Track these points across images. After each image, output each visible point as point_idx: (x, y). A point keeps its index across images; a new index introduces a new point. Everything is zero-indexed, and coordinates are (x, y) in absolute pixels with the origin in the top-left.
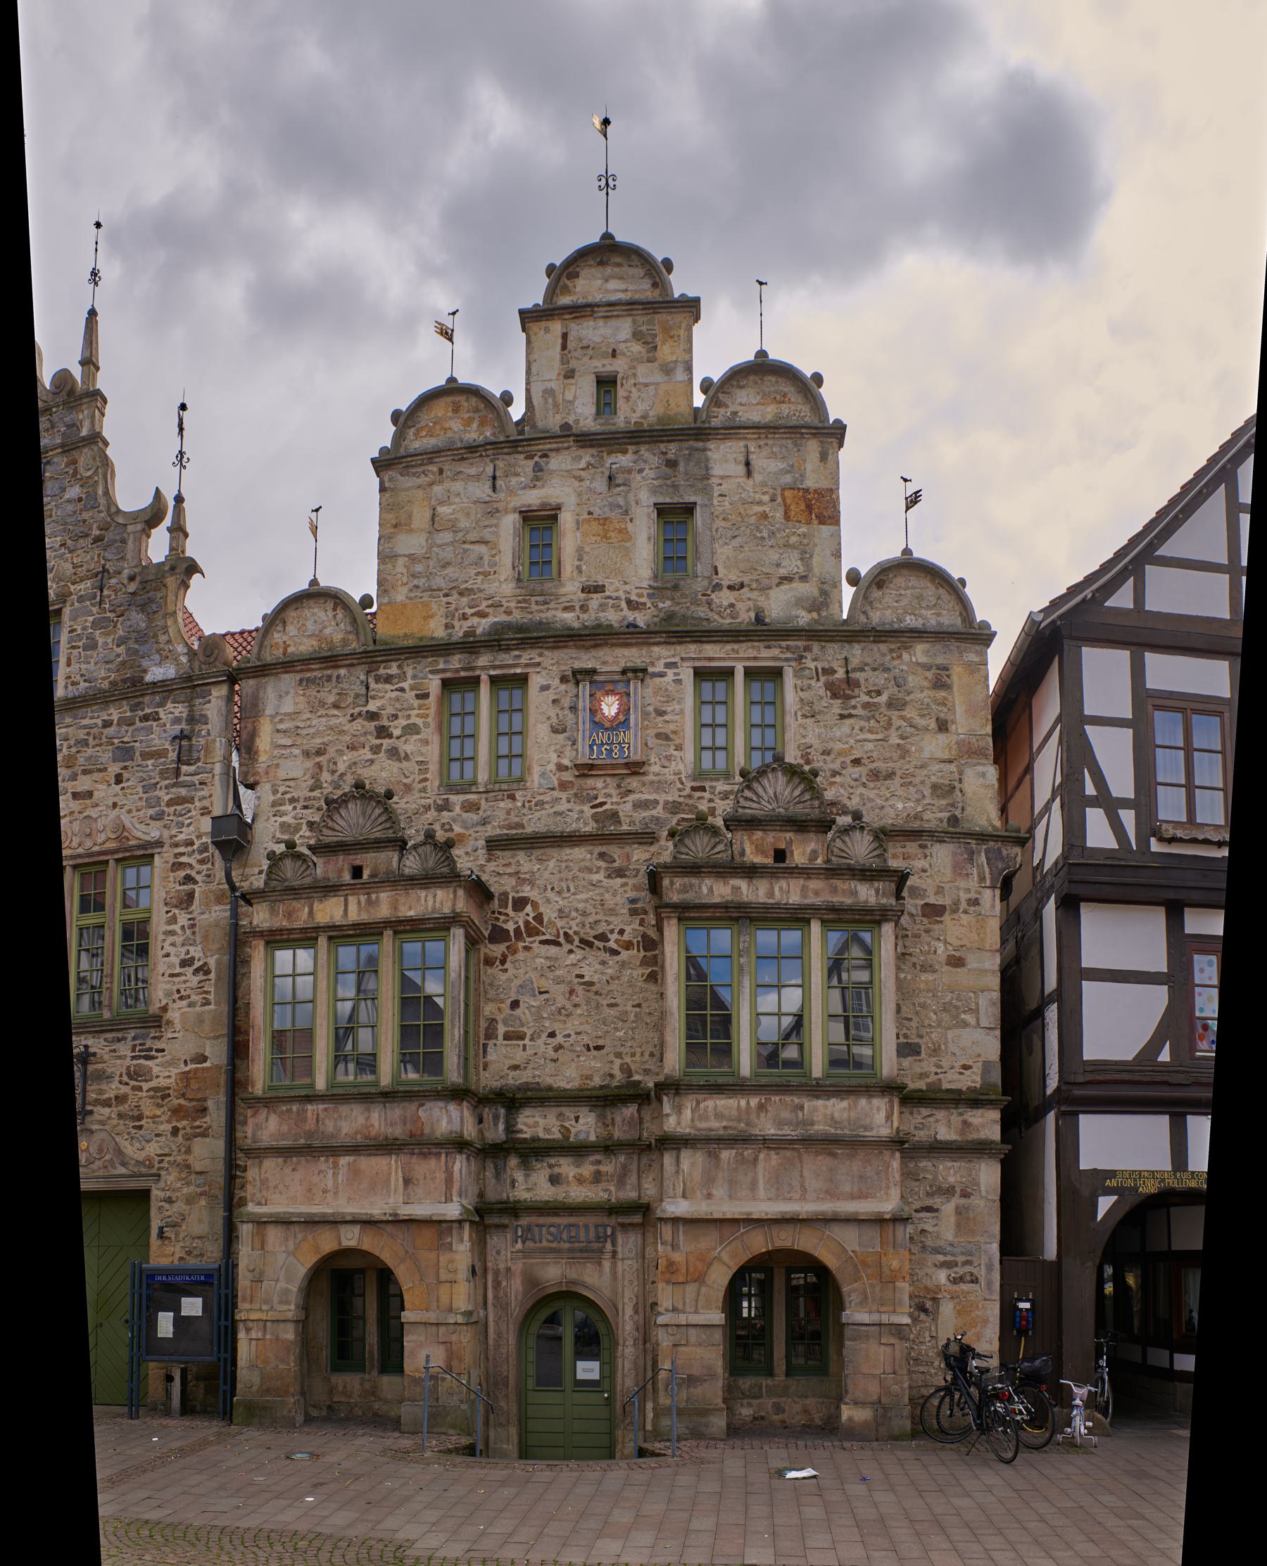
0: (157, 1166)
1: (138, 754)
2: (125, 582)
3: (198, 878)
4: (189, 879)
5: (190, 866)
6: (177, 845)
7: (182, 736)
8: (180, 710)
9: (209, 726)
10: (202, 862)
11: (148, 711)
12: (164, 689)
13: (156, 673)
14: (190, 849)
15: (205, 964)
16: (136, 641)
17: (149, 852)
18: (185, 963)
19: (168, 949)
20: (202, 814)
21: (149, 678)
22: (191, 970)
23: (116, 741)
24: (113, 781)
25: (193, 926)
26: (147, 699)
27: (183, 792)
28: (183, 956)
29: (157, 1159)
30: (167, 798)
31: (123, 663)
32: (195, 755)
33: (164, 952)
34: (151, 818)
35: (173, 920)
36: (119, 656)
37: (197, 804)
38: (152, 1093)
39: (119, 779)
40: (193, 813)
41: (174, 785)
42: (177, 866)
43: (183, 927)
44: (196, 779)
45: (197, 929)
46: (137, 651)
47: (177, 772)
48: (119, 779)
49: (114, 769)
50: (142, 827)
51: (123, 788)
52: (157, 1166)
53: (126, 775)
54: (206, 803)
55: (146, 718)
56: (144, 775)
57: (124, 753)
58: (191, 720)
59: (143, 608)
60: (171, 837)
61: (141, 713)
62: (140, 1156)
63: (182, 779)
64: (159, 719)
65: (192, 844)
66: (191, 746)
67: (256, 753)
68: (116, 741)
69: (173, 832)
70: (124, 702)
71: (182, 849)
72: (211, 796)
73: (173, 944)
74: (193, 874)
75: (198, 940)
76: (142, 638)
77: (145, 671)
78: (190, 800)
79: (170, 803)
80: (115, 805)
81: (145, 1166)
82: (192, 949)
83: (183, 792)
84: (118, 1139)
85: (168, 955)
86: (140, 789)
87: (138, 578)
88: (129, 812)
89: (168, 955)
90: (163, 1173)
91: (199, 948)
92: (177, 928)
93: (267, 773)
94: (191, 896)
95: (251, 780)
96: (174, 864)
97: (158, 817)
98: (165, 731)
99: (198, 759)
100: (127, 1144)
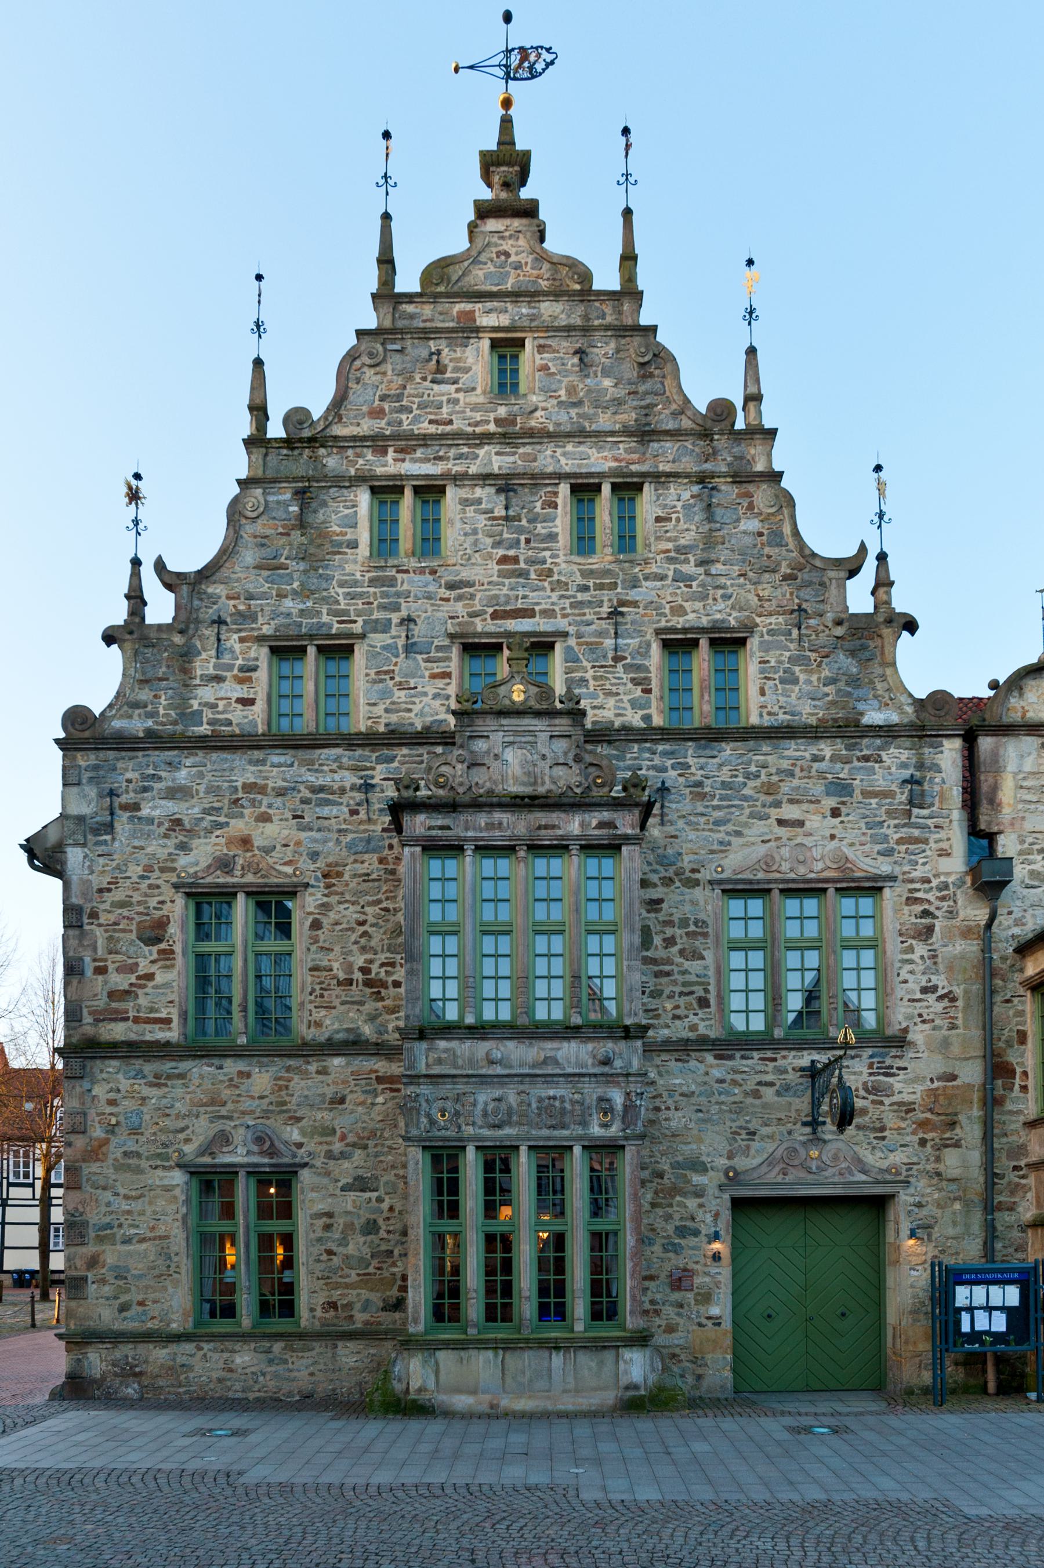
0: (904, 1173)
1: (857, 792)
2: (830, 625)
3: (937, 913)
4: (926, 913)
5: (928, 901)
6: (912, 881)
7: (911, 781)
8: (905, 755)
9: (943, 775)
10: (943, 899)
11: (865, 752)
12: (888, 733)
13: (874, 717)
14: (926, 886)
15: (950, 992)
16: (847, 684)
17: (879, 884)
18: (925, 990)
19: (904, 975)
20: (940, 855)
21: (866, 720)
22: (934, 996)
23: (829, 776)
24: (828, 813)
25: (935, 956)
26: (865, 741)
27: (916, 833)
28: (924, 984)
29: (905, 1167)
30: (896, 836)
31: (833, 703)
32: (928, 800)
33: (901, 978)
34: (879, 853)
35: (911, 950)
36: (827, 695)
37: (933, 845)
38: (895, 1107)
39: (835, 813)
40: (928, 853)
41: (905, 825)
42: (911, 901)
43: (922, 957)
44: (929, 822)
45: (939, 960)
46: (849, 694)
47: (909, 814)
48: (835, 813)
49: (831, 802)
50: (868, 860)
51: (842, 822)
52: (904, 1173)
53: (844, 810)
54: (944, 845)
55: (866, 759)
56: (868, 813)
57: (841, 788)
58: (920, 766)
59: (852, 653)
60: (904, 873)
61: (859, 754)
62: (884, 1164)
63: (913, 820)
64: (881, 761)
65: (929, 882)
66: (923, 791)
67: (1000, 804)
68: (829, 776)
69: (906, 868)
70: (838, 740)
71: (917, 886)
72: (948, 839)
73: (911, 972)
74: (932, 909)
75: (941, 967)
76: (854, 682)
77: (862, 714)
78: (926, 841)
79: (899, 842)
80: (833, 837)
81: (890, 1173)
82: (933, 978)
83: (916, 833)
84: (856, 1148)
85: (906, 982)
86: (863, 826)
87: (846, 625)
88: (852, 845)
89: (906, 982)
90: (911, 1179)
91: (943, 977)
92: (915, 957)
93: (1012, 824)
94: (930, 930)
95: (995, 829)
96: (908, 899)
97: (888, 853)
98: (890, 774)
99: (932, 805)
100: (867, 1153)
